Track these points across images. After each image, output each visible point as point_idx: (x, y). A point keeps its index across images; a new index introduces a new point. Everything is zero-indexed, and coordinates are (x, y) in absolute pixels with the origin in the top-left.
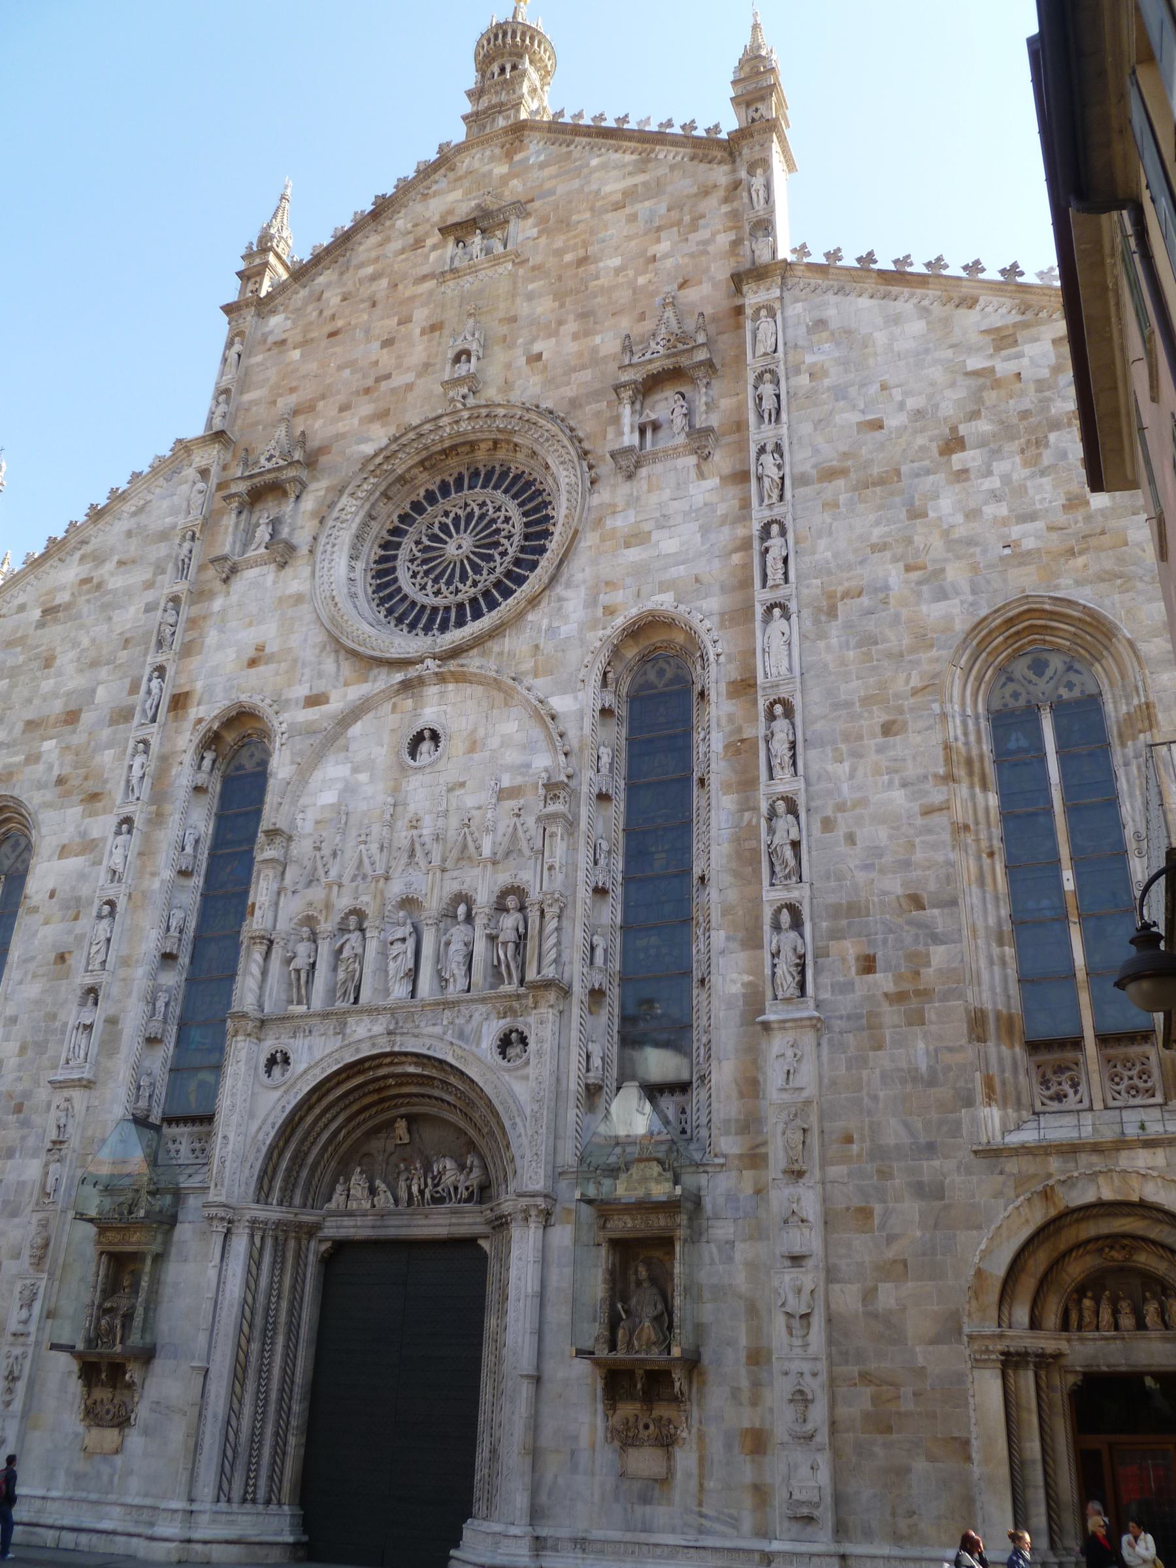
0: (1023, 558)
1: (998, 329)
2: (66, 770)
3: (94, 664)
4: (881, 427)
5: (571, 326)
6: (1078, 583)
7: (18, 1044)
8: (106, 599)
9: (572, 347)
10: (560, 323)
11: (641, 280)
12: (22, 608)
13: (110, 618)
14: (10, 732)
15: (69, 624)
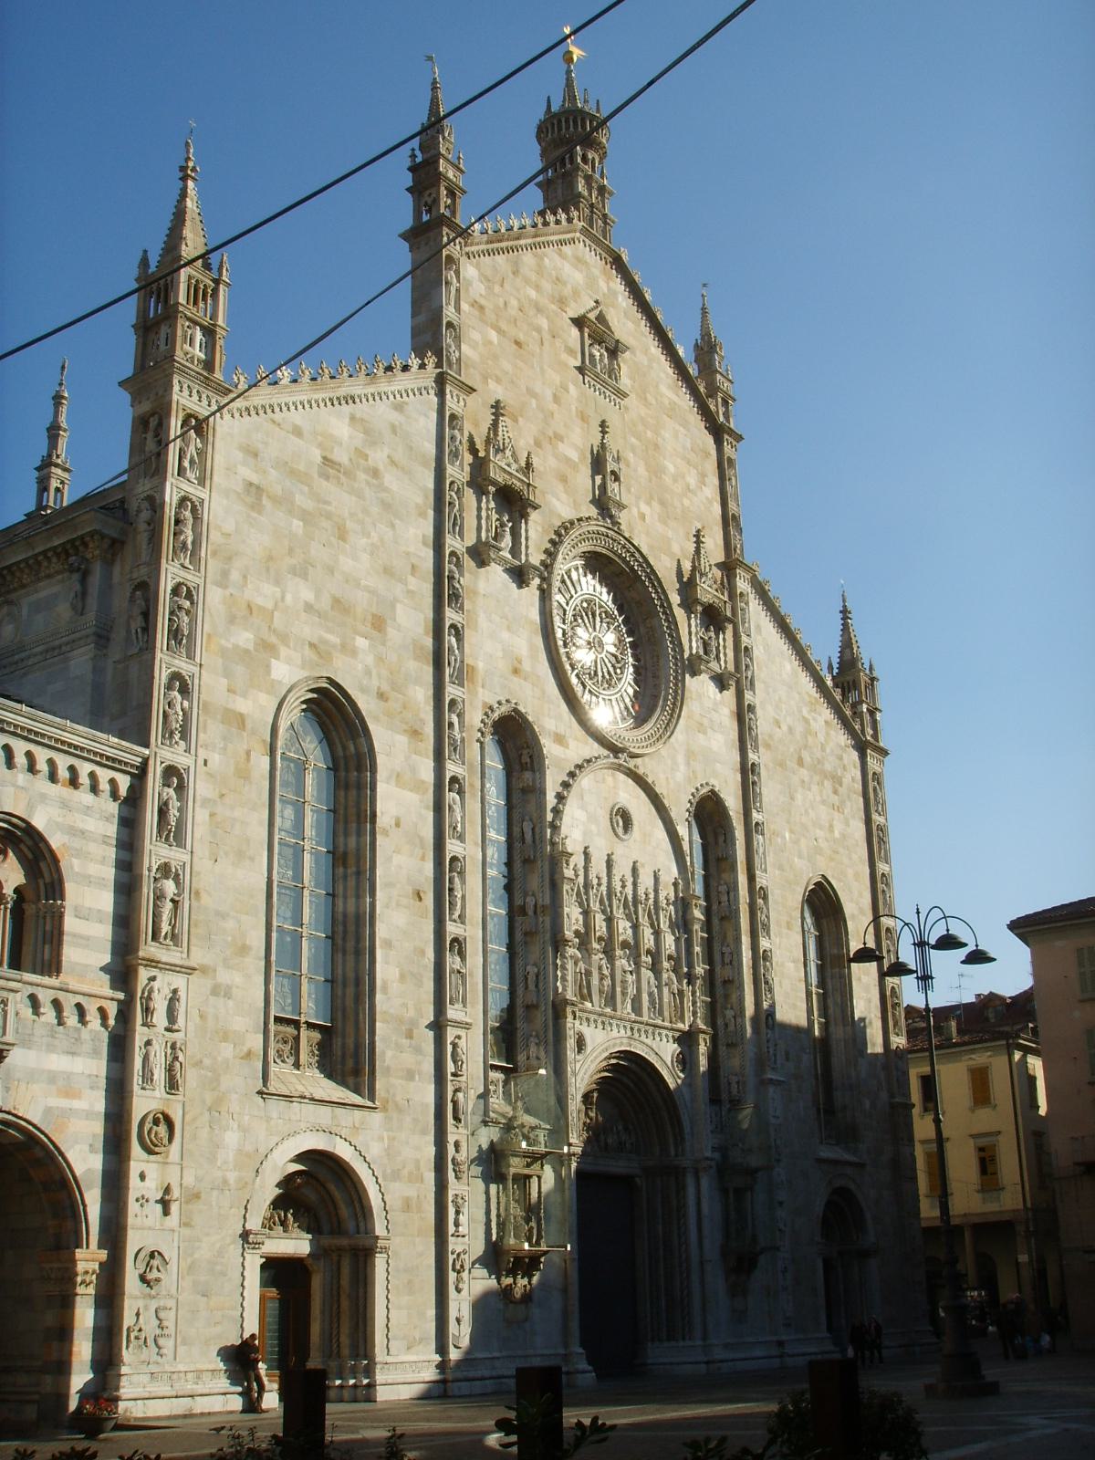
0: (818, 850)
1: (810, 696)
2: (385, 687)
3: (388, 571)
4: (780, 727)
5: (655, 504)
6: (833, 876)
7: (397, 969)
8: (384, 495)
9: (660, 528)
10: (652, 498)
11: (686, 502)
12: (298, 432)
13: (393, 526)
14: (318, 593)
15: (354, 498)
